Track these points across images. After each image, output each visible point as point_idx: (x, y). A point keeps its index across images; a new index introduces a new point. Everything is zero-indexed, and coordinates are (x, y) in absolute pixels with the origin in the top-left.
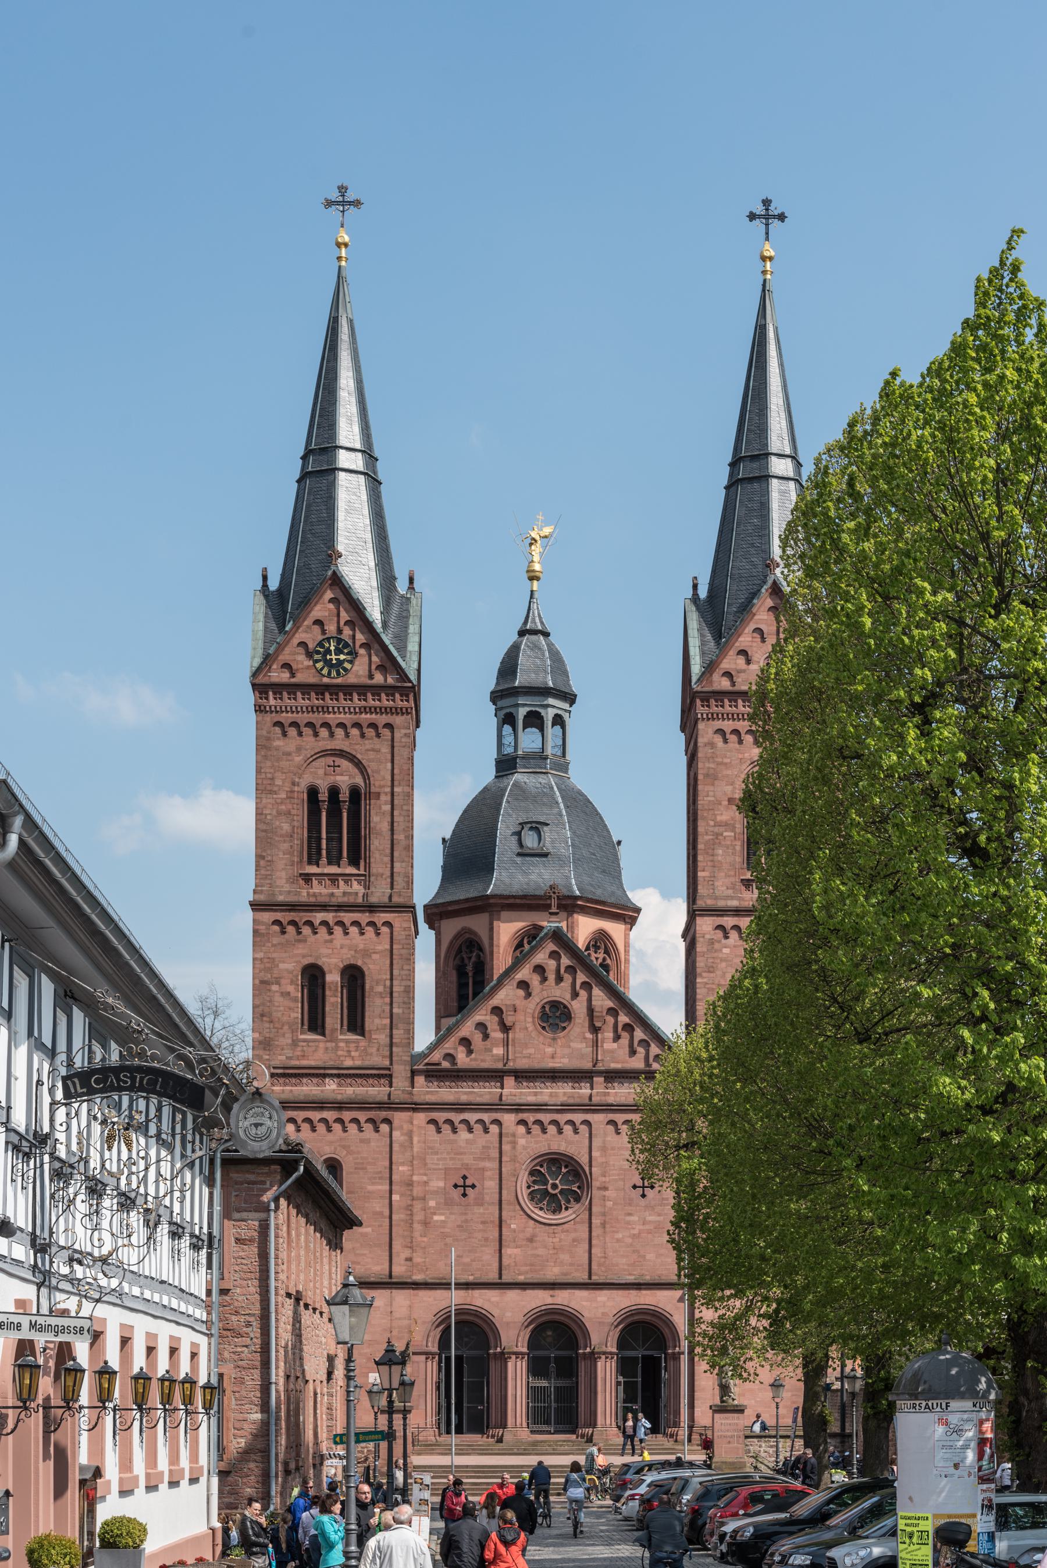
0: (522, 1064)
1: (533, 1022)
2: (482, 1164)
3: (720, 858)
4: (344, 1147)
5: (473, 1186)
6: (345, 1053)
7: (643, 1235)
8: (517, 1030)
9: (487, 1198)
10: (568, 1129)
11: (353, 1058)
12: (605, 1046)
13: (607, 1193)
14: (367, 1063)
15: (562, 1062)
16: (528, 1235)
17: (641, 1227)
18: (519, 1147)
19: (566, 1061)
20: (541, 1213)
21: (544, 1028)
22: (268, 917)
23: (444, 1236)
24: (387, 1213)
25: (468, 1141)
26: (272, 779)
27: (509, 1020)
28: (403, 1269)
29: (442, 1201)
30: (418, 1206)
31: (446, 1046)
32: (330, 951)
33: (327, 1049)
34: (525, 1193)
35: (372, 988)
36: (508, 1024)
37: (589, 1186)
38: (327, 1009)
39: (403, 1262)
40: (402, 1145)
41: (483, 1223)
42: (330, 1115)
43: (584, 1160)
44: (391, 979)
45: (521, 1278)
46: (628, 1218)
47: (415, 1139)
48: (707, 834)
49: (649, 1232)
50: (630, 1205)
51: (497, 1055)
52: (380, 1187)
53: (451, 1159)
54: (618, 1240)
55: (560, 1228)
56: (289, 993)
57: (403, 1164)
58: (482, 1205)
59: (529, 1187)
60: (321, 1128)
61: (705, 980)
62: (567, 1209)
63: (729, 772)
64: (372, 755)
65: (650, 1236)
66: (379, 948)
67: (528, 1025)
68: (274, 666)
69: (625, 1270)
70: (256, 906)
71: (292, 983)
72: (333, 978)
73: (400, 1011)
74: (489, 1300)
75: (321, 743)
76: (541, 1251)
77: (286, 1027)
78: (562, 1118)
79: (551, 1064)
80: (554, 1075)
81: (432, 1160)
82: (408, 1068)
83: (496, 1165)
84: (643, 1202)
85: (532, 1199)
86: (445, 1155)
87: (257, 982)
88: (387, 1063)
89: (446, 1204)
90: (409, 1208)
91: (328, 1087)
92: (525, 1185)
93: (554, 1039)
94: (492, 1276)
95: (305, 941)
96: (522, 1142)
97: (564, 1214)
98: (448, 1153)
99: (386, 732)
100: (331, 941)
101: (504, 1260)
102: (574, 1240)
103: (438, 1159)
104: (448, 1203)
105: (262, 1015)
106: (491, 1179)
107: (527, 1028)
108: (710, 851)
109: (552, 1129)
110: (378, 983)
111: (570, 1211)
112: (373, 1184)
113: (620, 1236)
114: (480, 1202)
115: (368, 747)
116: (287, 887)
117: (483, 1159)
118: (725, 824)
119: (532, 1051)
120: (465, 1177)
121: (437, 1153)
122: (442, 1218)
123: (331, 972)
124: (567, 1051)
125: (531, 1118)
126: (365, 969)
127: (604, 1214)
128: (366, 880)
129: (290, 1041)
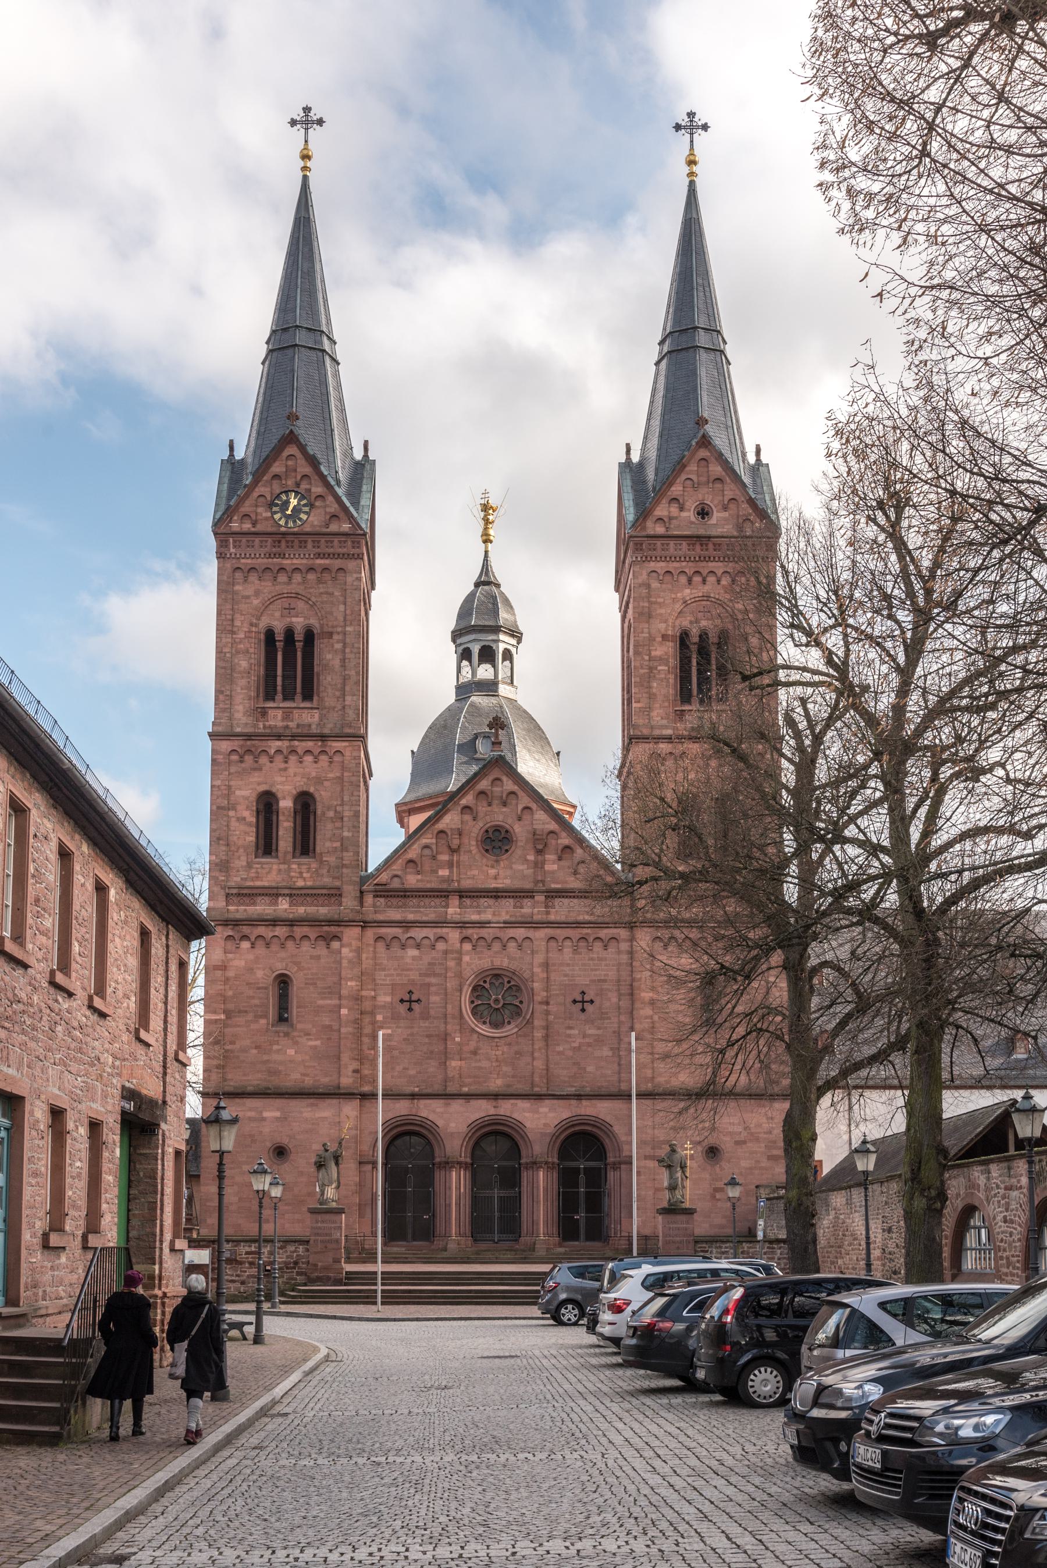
0: (467, 884)
1: (477, 845)
2: (427, 980)
4: (295, 963)
7: (584, 1048)
9: (432, 1012)
11: (305, 879)
12: (547, 867)
14: (318, 883)
15: (504, 882)
16: (472, 1048)
18: (464, 965)
19: (508, 881)
20: (483, 1027)
21: (487, 851)
22: (225, 746)
25: (414, 958)
26: (232, 620)
28: (351, 1080)
29: (389, 1014)
30: (367, 1019)
31: (394, 867)
32: (284, 779)
33: (280, 870)
35: (324, 814)
38: (280, 833)
39: (350, 1074)
40: (350, 962)
41: (428, 1036)
45: (465, 1089)
46: (568, 1032)
47: (364, 956)
48: (642, 668)
49: (589, 1045)
50: (570, 1018)
51: (443, 876)
52: (329, 1002)
53: (398, 975)
54: (559, 1053)
55: (503, 1041)
56: (244, 819)
57: (351, 979)
58: (427, 1019)
59: (472, 1002)
62: (509, 1023)
63: (663, 611)
64: (325, 598)
65: (590, 1049)
66: (331, 775)
68: (235, 518)
69: (565, 1082)
70: (212, 735)
71: (247, 808)
72: (286, 804)
74: (434, 1112)
75: (278, 588)
76: (485, 1064)
77: (241, 850)
79: (493, 885)
80: (496, 894)
81: (380, 976)
82: (357, 888)
84: (582, 1016)
86: (392, 972)
87: (215, 808)
93: (497, 861)
95: (260, 769)
96: (466, 958)
98: (395, 969)
100: (285, 769)
102: (517, 1053)
104: (395, 1017)
105: (219, 839)
107: (470, 851)
110: (329, 809)
111: (512, 1026)
112: (322, 999)
115: (322, 590)
116: (244, 720)
118: (661, 660)
119: (476, 872)
121: (384, 970)
123: (284, 798)
124: (509, 872)
125: (474, 933)
126: (317, 796)
129: (244, 863)
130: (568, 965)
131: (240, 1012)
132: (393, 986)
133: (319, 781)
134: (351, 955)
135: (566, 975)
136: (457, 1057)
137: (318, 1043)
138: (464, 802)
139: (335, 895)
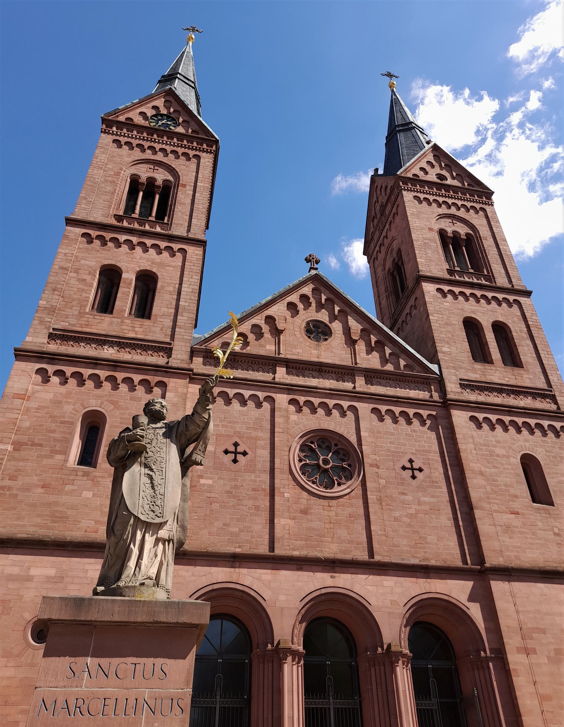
2: (254, 434)
3: (429, 255)
5: (245, 454)
6: (129, 328)
8: (288, 335)
9: (259, 466)
13: (380, 471)
16: (302, 507)
17: (417, 507)
21: (309, 337)
27: (280, 326)
33: (112, 323)
34: (298, 465)
35: (163, 287)
36: (279, 328)
37: (361, 463)
41: (254, 490)
42: (103, 374)
43: (353, 439)
44: (181, 284)
50: (403, 484)
51: (269, 350)
53: (223, 426)
54: (396, 519)
55: (334, 502)
58: (254, 472)
59: (300, 460)
60: (90, 384)
61: (436, 318)
62: (339, 484)
73: (187, 304)
74: (259, 579)
78: (331, 402)
83: (268, 435)
84: (414, 482)
85: (303, 474)
88: (168, 340)
92: (297, 459)
93: (318, 345)
94: (263, 550)
97: (336, 488)
99: (194, 160)
102: (350, 516)
106: (263, 448)
108: (423, 250)
109: (321, 411)
110: (169, 284)
111: (343, 487)
114: (251, 468)
122: (210, 482)
123: (127, 272)
128: (169, 225)
129: (76, 313)
130: (392, 434)
131: (34, 444)
134: (176, 399)
135: (391, 443)
136: (286, 514)
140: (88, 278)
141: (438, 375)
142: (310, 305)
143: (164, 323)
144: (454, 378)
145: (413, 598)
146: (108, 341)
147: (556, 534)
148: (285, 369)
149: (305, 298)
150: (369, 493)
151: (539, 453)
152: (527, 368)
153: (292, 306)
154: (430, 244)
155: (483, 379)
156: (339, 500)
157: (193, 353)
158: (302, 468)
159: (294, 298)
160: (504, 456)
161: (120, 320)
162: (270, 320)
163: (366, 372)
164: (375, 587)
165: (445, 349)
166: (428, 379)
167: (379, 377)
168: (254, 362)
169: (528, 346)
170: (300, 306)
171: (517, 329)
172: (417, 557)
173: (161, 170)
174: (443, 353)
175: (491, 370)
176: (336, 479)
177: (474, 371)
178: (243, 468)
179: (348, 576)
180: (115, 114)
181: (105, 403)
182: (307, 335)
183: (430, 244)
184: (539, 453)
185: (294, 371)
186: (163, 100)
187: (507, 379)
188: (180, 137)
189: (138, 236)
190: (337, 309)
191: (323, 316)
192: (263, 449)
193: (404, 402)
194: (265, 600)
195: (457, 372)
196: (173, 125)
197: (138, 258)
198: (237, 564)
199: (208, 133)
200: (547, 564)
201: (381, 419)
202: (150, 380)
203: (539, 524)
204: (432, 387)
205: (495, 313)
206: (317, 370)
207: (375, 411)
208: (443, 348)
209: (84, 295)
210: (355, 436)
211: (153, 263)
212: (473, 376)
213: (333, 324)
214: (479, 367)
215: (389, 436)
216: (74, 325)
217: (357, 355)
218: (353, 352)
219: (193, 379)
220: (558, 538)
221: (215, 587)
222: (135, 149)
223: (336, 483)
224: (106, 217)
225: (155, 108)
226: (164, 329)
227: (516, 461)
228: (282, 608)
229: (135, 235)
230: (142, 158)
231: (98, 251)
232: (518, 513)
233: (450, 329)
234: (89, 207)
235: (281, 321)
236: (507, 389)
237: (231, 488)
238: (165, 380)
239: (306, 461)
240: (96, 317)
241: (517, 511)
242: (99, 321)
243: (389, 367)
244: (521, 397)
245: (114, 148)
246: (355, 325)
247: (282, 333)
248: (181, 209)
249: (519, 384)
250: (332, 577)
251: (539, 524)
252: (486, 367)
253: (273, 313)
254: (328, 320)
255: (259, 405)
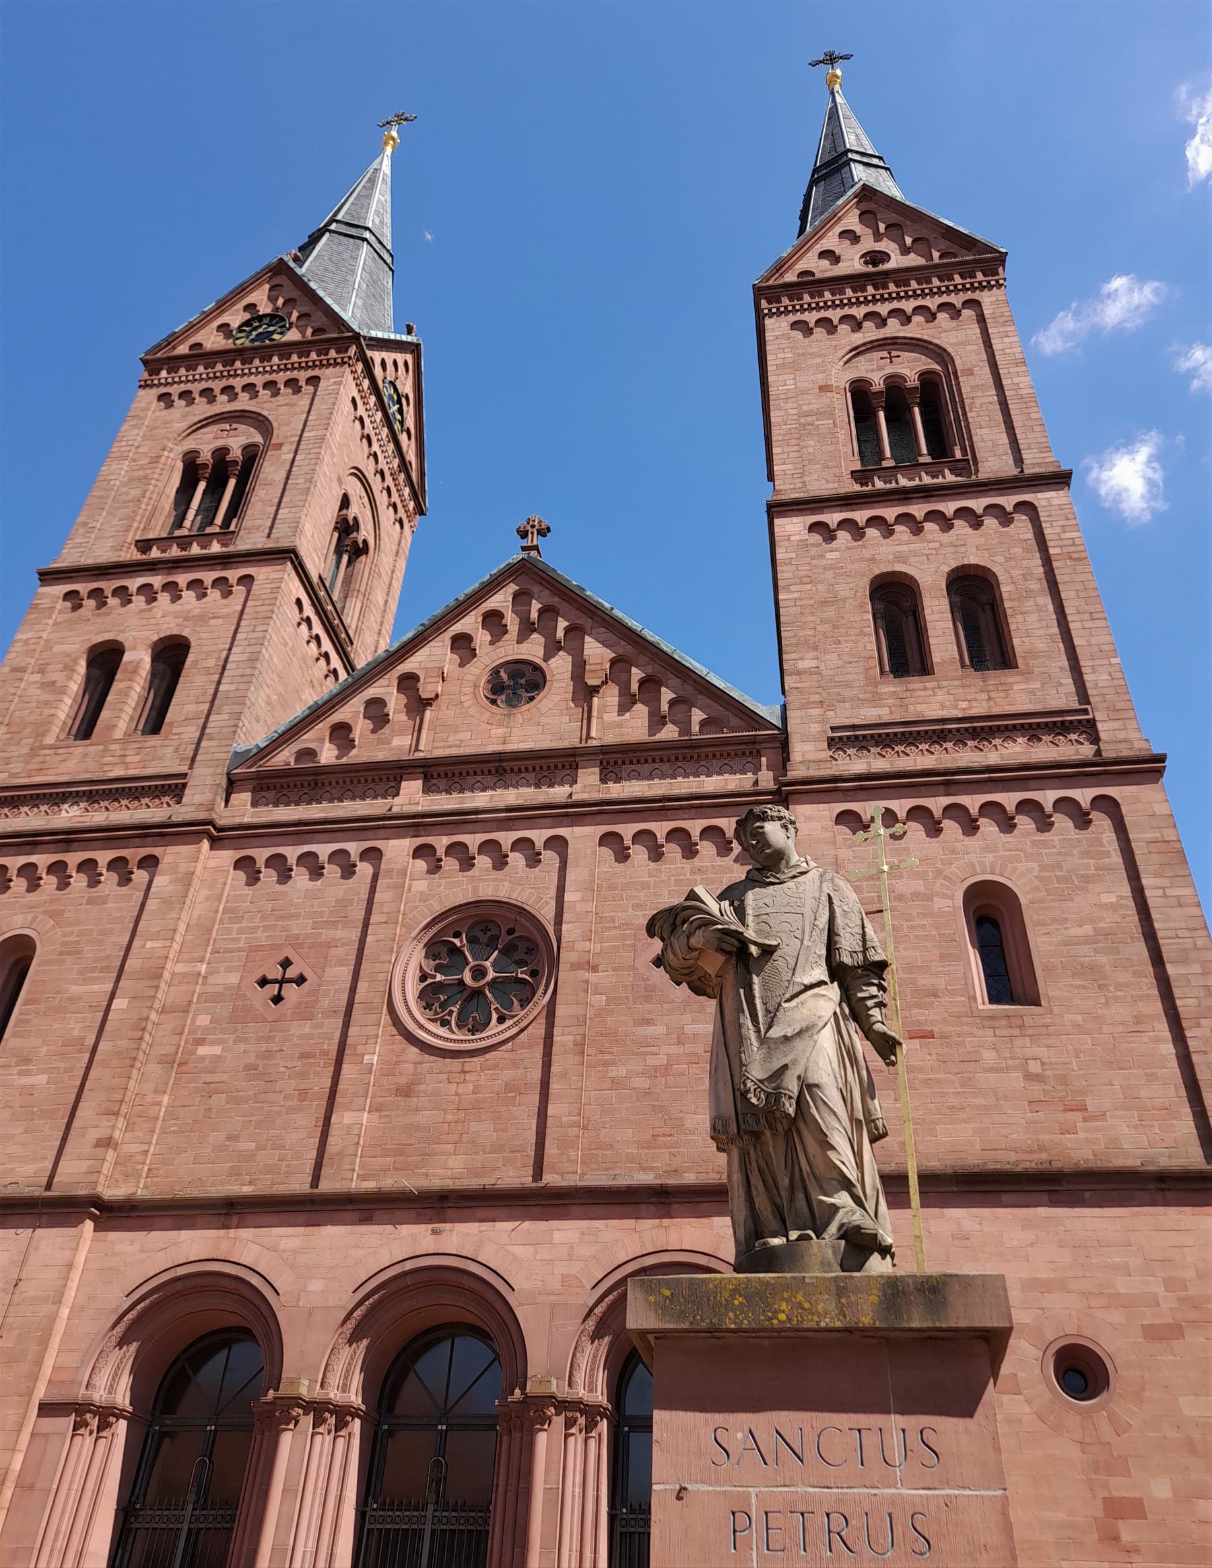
2: (326, 934)
3: (811, 450)
6: (115, 760)
7: (677, 1068)
8: (444, 707)
9: (325, 1002)
10: (517, 860)
16: (403, 1080)
17: (674, 1049)
21: (494, 702)
23: (210, 1090)
24: (90, 1041)
25: (309, 895)
28: (84, 1166)
34: (413, 988)
35: (196, 662)
37: (554, 964)
38: (110, 698)
39: (88, 1150)
41: (304, 1056)
43: (546, 914)
50: (648, 999)
51: (399, 748)
52: (96, 987)
54: (616, 1084)
59: (423, 978)
61: (795, 595)
62: (501, 1020)
67: (463, 699)
73: (233, 687)
74: (274, 1248)
76: (421, 1118)
78: (506, 838)
83: (355, 934)
85: (428, 1006)
86: (257, 922)
88: (184, 769)
89: (234, 1020)
90: (141, 1025)
91: (64, 814)
93: (509, 715)
97: (494, 1027)
100: (150, 610)
101: (331, 1140)
102: (508, 1087)
103: (240, 931)
104: (241, 1015)
111: (509, 1023)
112: (86, 981)
113: (620, 1071)
114: (305, 1013)
117: (333, 925)
120: (286, 963)
122: (217, 1050)
123: (134, 648)
127: (582, 1021)
132: (254, 949)
133: (202, 618)
134: (170, 888)
137: (42, 1079)
138: (457, 628)
139: (173, 787)
140: (59, 677)
141: (778, 729)
142: (504, 630)
143: (183, 736)
144: (815, 728)
145: (619, 1266)
146: (70, 793)
147: (1029, 1077)
148: (420, 782)
149: (493, 620)
150: (557, 1031)
151: (1022, 875)
152: (1027, 665)
153: (462, 644)
154: (817, 423)
155: (898, 718)
156: (487, 1056)
157: (232, 785)
158: (422, 995)
159: (470, 623)
160: (916, 896)
161: (101, 748)
162: (408, 682)
163: (604, 754)
164: (531, 1248)
165: (803, 665)
166: (755, 743)
167: (635, 761)
168: (355, 781)
169: (1040, 609)
170: (482, 637)
171: (1016, 573)
172: (652, 1169)
173: (242, 427)
174: (798, 673)
175: (925, 689)
176: (496, 1009)
177: (875, 699)
178: (290, 1012)
179: (471, 1228)
180: (169, 344)
181: (40, 917)
182: (487, 698)
183: (817, 423)
184: (1022, 875)
185: (442, 784)
186: (267, 286)
187: (964, 705)
188: (302, 347)
189: (166, 571)
190: (562, 624)
191: (533, 649)
192: (341, 965)
193: (681, 808)
194: (278, 1294)
195: (831, 713)
196: (279, 330)
197: (159, 616)
198: (235, 1219)
199: (343, 325)
200: (1000, 1155)
201: (622, 856)
202: (129, 858)
203: (988, 1056)
204: (764, 760)
205: (962, 549)
206: (493, 771)
207: (609, 839)
208: (800, 662)
209: (47, 712)
210: (553, 903)
211: (186, 619)
212: (869, 714)
213: (552, 660)
214: (892, 689)
215: (635, 893)
216: (16, 775)
217: (594, 721)
218: (586, 716)
219: (220, 839)
220: (1037, 1087)
221: (181, 1271)
222: (196, 401)
223: (495, 1016)
224: (117, 550)
225: (250, 307)
226: (182, 748)
227: (952, 904)
228: (311, 1311)
229: (160, 572)
230: (208, 415)
231: (89, 620)
232: (931, 1035)
233: (830, 612)
234: (87, 540)
235: (429, 680)
236: (958, 730)
237: (258, 1057)
238: (157, 851)
239: (434, 977)
240: (59, 751)
241: (929, 1029)
242: (62, 757)
243: (670, 732)
244: (997, 741)
245: (160, 410)
246: (597, 652)
247: (431, 705)
248: (263, 496)
249: (996, 711)
250: (434, 1232)
251: (988, 1056)
252: (910, 686)
253: (417, 665)
254: (541, 653)
255: (348, 871)
